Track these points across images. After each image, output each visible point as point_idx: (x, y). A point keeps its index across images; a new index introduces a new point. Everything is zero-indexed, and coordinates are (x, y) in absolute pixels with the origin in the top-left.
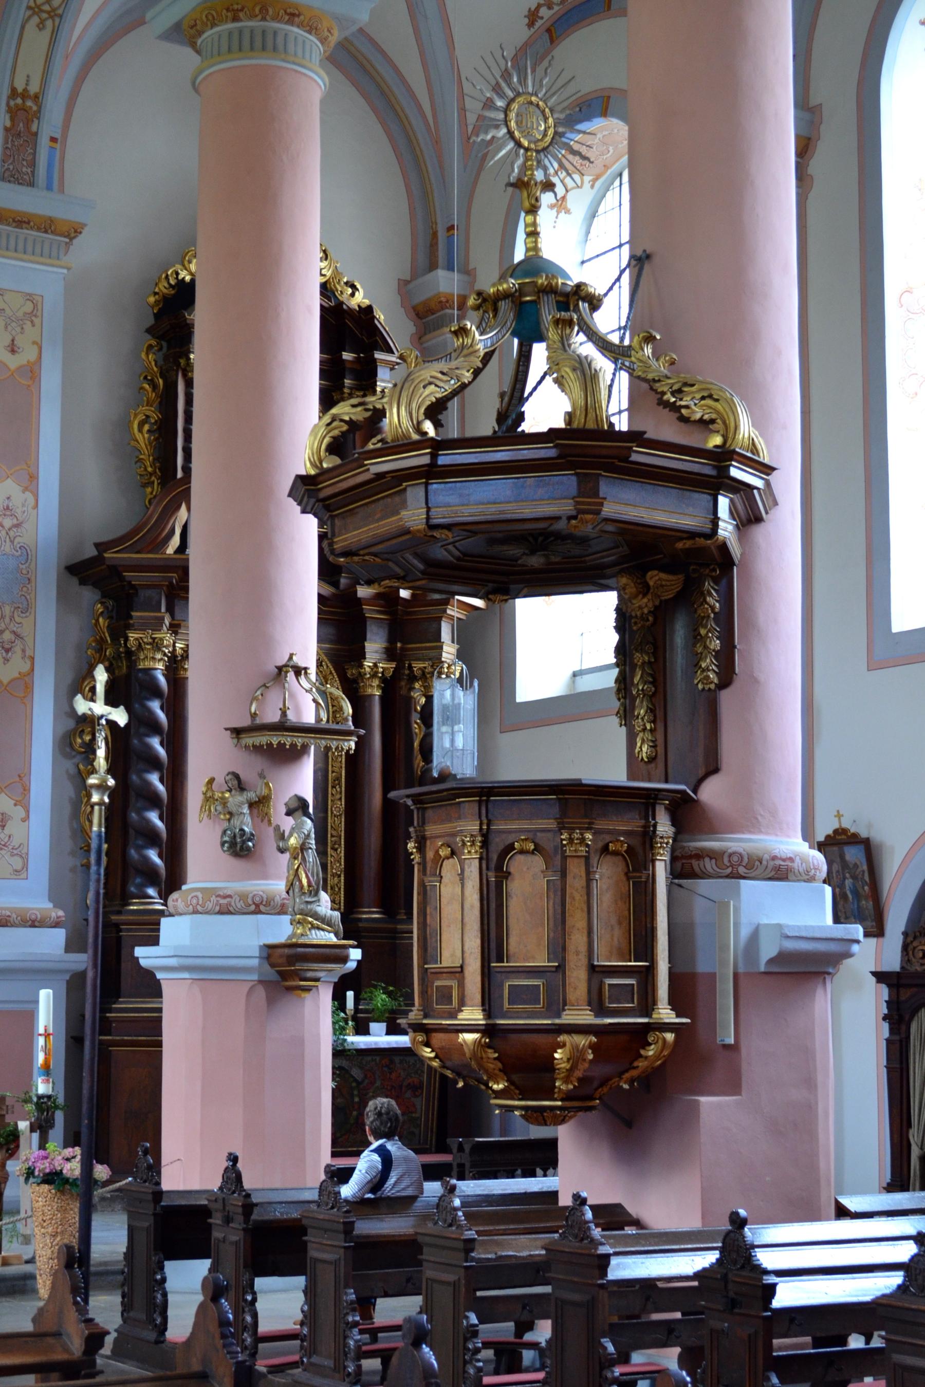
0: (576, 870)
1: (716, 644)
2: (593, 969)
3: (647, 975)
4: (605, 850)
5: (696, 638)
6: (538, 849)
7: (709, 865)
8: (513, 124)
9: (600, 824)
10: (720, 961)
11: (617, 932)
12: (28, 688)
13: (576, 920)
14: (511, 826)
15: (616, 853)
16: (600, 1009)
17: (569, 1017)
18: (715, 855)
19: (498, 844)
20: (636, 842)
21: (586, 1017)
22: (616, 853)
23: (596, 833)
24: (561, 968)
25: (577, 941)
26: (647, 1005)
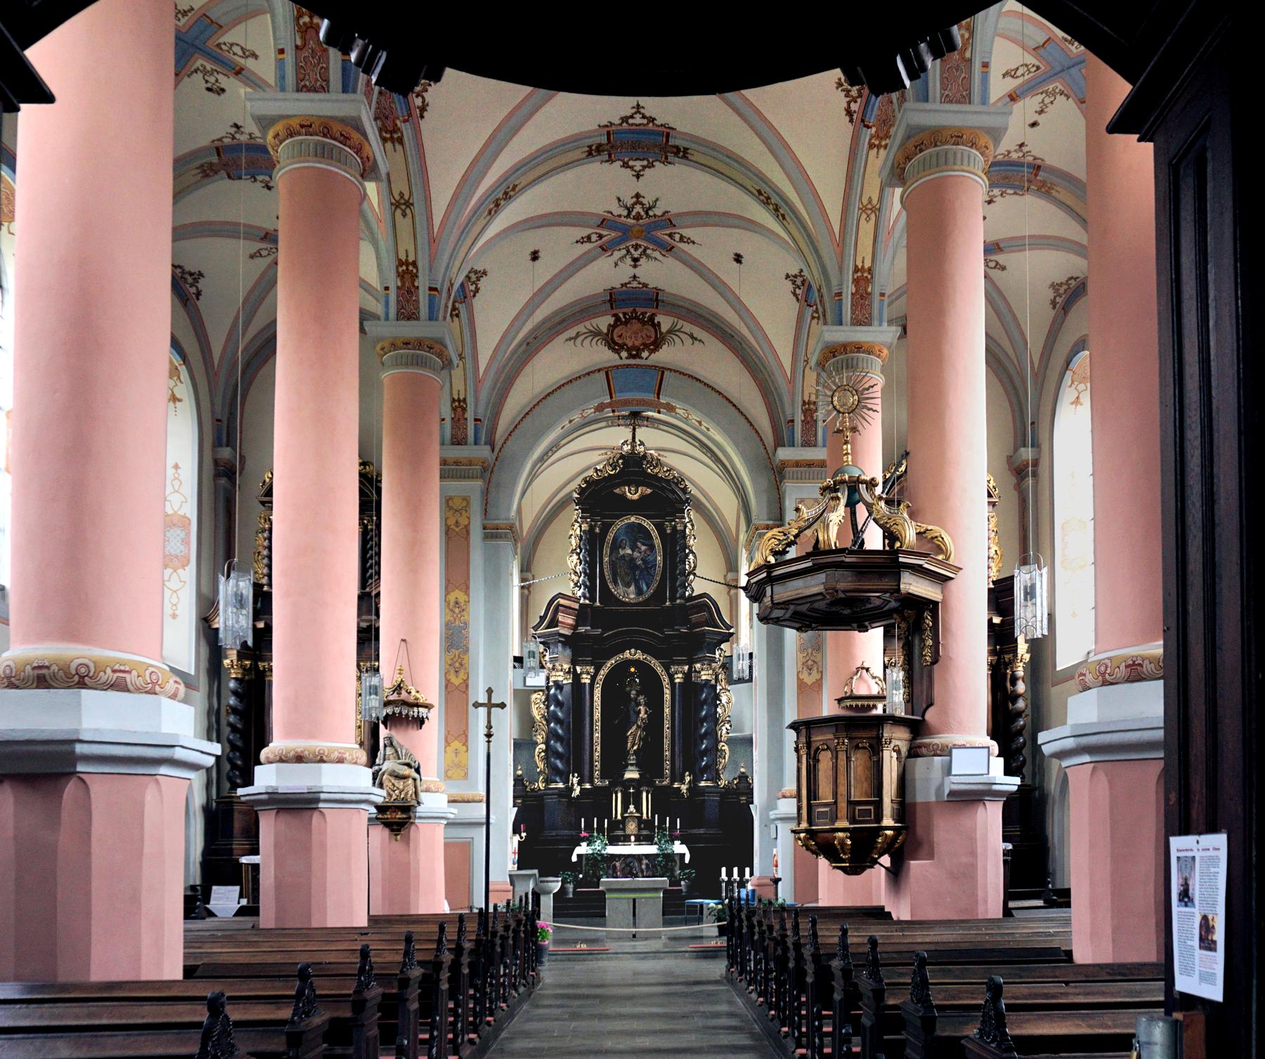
0: (842, 756)
1: (930, 642)
2: (850, 802)
3: (879, 805)
4: (857, 747)
5: (923, 641)
6: (828, 748)
7: (924, 750)
8: (835, 403)
9: (854, 734)
10: (924, 793)
11: (865, 785)
12: (820, 686)
13: (842, 780)
14: (818, 738)
15: (864, 748)
16: (853, 821)
17: (838, 825)
18: (926, 746)
19: (814, 746)
20: (874, 742)
21: (844, 824)
22: (864, 748)
23: (850, 739)
24: (836, 803)
25: (842, 790)
26: (879, 817)
